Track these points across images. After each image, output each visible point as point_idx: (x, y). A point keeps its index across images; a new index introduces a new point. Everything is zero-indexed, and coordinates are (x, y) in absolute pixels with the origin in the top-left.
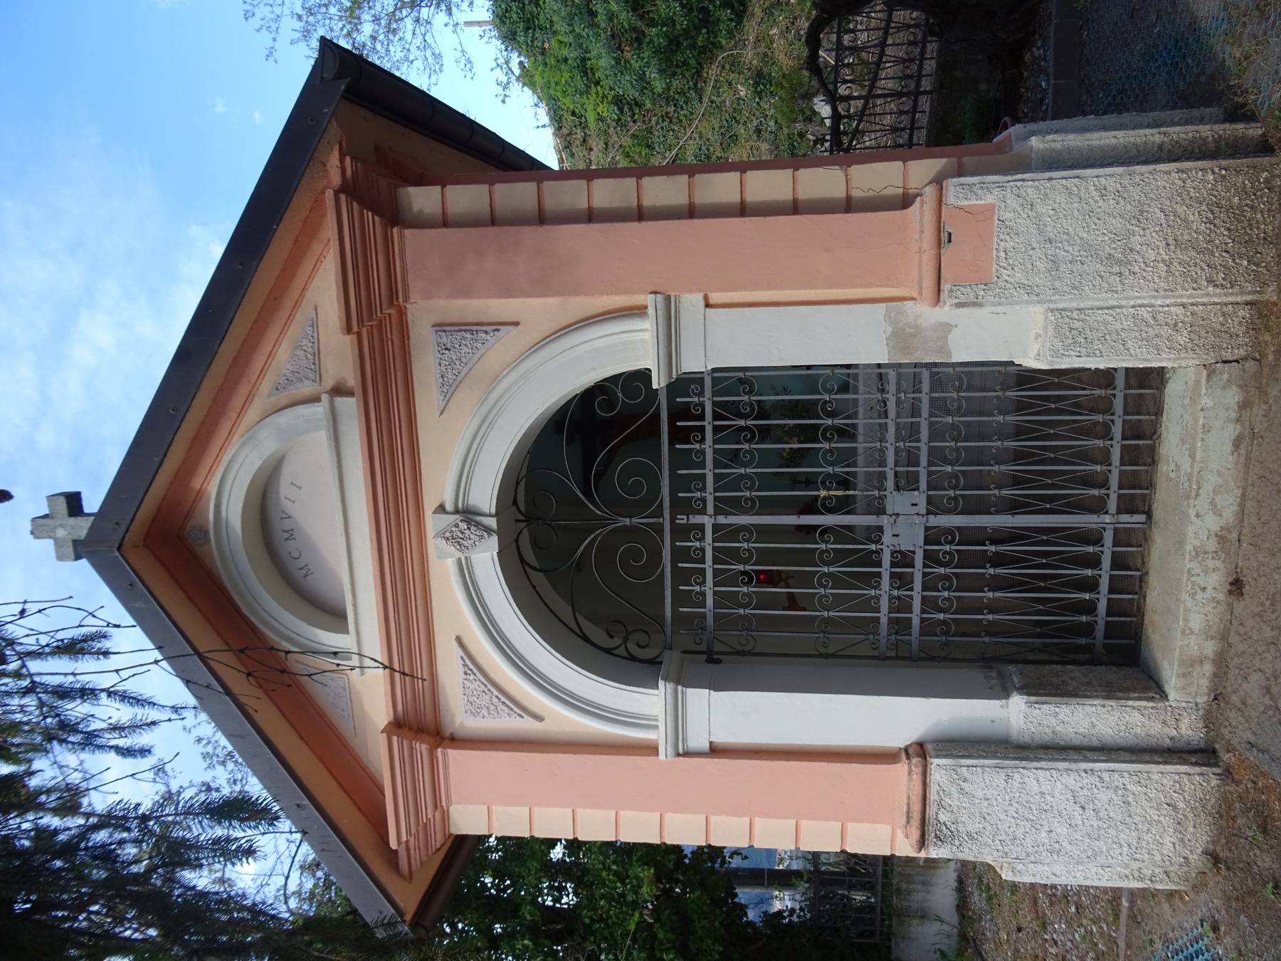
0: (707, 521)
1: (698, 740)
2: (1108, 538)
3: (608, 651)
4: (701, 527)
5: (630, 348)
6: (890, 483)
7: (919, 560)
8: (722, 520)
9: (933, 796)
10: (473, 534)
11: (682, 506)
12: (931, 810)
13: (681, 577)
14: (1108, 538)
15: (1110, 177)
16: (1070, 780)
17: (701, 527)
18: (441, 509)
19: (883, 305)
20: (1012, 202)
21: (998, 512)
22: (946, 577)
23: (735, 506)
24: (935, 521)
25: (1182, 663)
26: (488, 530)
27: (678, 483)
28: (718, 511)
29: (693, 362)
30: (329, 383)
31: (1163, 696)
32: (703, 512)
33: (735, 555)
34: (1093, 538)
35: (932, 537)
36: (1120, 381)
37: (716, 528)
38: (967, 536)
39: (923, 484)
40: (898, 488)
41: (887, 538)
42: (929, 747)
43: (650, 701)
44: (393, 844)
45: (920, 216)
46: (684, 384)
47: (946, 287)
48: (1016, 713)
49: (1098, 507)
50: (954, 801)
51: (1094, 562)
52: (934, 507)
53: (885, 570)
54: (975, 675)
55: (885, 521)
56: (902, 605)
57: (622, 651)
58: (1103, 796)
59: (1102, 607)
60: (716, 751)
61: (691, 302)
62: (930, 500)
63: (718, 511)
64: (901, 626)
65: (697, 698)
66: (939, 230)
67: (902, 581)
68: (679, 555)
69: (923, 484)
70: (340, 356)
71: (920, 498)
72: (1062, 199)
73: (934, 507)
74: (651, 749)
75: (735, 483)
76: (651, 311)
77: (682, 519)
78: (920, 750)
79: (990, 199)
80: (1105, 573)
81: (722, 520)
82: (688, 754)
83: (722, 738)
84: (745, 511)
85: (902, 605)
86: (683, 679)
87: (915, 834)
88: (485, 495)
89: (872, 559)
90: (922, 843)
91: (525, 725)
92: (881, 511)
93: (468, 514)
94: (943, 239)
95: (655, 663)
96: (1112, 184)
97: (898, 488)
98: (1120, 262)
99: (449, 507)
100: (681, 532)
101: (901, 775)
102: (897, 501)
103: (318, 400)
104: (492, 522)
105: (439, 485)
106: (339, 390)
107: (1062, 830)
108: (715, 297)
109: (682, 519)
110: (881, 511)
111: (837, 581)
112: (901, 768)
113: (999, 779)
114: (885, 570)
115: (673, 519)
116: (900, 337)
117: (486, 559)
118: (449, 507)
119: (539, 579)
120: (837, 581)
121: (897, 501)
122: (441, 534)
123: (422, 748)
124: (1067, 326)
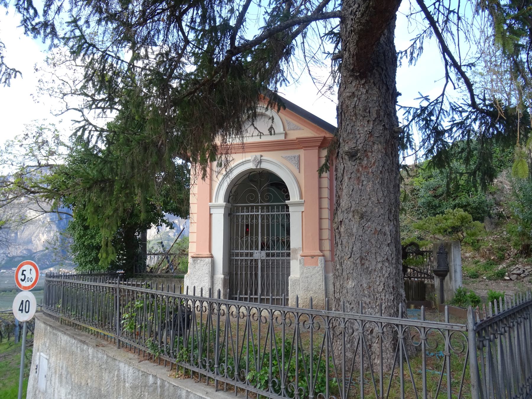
0: (259, 213)
3: (231, 192)
4: (258, 212)
5: (294, 196)
6: (268, 251)
8: (260, 216)
9: (203, 259)
10: (256, 163)
11: (263, 207)
12: (200, 259)
13: (247, 207)
14: (256, 297)
15: (323, 287)
17: (258, 212)
18: (261, 156)
20: (319, 269)
22: (248, 264)
23: (263, 219)
24: (259, 261)
26: (257, 166)
27: (268, 207)
28: (262, 215)
29: (291, 209)
30: (288, 132)
32: (261, 212)
33: (252, 219)
34: (256, 294)
35: (256, 260)
37: (258, 215)
38: (256, 268)
39: (268, 258)
40: (266, 253)
41: (256, 251)
43: (221, 201)
45: (318, 252)
50: (202, 263)
52: (262, 261)
53: (249, 251)
54: (227, 270)
56: (242, 255)
57: (231, 195)
60: (211, 215)
61: (302, 209)
63: (262, 215)
64: (237, 255)
65: (222, 211)
66: (314, 256)
67: (247, 255)
68: (252, 207)
69: (268, 258)
70: (294, 135)
71: (264, 258)
72: (319, 278)
73: (262, 261)
74: (211, 201)
75: (268, 219)
77: (260, 207)
78: (212, 257)
79: (319, 265)
81: (260, 216)
83: (213, 216)
84: (261, 221)
85: (242, 255)
86: (226, 208)
87: (195, 256)
88: (265, 166)
89: (251, 248)
90: (193, 257)
92: (262, 250)
93: (260, 162)
94: (313, 256)
95: (229, 202)
96: (321, 287)
97: (266, 253)
98: (307, 289)
99: (262, 158)
100: (257, 207)
101: (207, 253)
102: (264, 253)
103: (284, 130)
104: (258, 167)
105: (267, 156)
106: (286, 134)
108: (304, 213)
109: (260, 207)
110: (262, 250)
111: (247, 241)
112: (208, 253)
113: (207, 272)
114: (249, 251)
115: (260, 206)
116: (296, 250)
117: (251, 166)
118: (262, 158)
119: (247, 176)
120: (247, 241)
124: (296, 281)
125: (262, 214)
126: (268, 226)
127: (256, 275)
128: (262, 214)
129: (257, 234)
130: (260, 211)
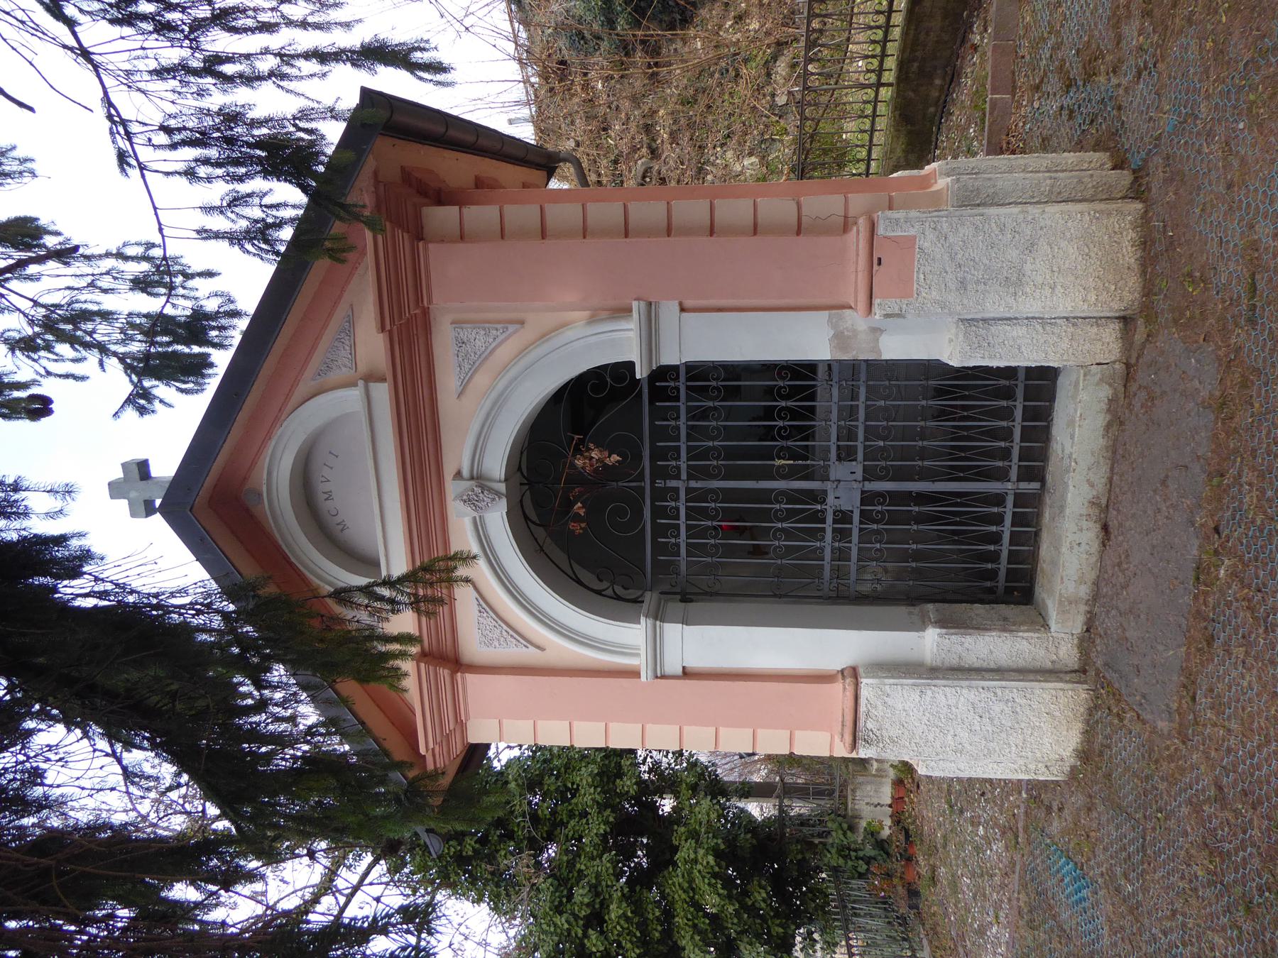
1: (673, 664)
2: (1010, 501)
3: (599, 593)
4: (676, 490)
5: (621, 343)
7: (856, 517)
8: (693, 484)
9: (862, 709)
10: (486, 497)
11: (659, 473)
13: (658, 531)
14: (1010, 501)
16: (972, 695)
17: (676, 490)
18: (458, 475)
19: (827, 313)
20: (931, 235)
21: (920, 480)
22: (878, 532)
23: (706, 474)
25: (1061, 602)
26: (498, 493)
27: (657, 454)
28: (690, 477)
29: (669, 357)
30: (362, 368)
31: (1046, 626)
32: (678, 477)
33: (704, 513)
34: (999, 500)
35: (867, 498)
36: (1021, 375)
37: (689, 490)
38: (896, 497)
39: (860, 456)
40: (839, 459)
41: (830, 499)
42: (861, 671)
44: (422, 751)
45: (856, 240)
46: (662, 373)
47: (876, 301)
48: (929, 642)
49: (1002, 475)
50: (879, 712)
51: (999, 519)
52: (869, 475)
53: (829, 526)
54: (901, 611)
55: (829, 486)
56: (841, 555)
57: (609, 592)
58: (997, 707)
59: (1004, 555)
60: (687, 674)
61: (669, 310)
62: (865, 469)
63: (690, 477)
64: (839, 573)
65: (672, 631)
67: (842, 534)
68: (658, 512)
69: (860, 456)
70: (371, 344)
71: (858, 468)
73: (869, 475)
74: (634, 674)
76: (635, 314)
77: (660, 483)
78: (853, 673)
79: (912, 232)
80: (1007, 528)
81: (693, 484)
82: (663, 677)
83: (694, 663)
85: (841, 555)
86: (659, 616)
87: (848, 738)
88: (496, 464)
89: (819, 517)
90: (854, 746)
91: (527, 655)
92: (825, 478)
94: (874, 261)
95: (637, 601)
97: (839, 459)
99: (466, 473)
100: (659, 494)
101: (838, 693)
103: (355, 385)
104: (502, 487)
105: (457, 456)
106: (370, 378)
107: (964, 735)
108: (689, 303)
109: (660, 483)
110: (825, 478)
111: (789, 534)
112: (838, 686)
113: (915, 695)
114: (829, 526)
115: (653, 482)
117: (497, 519)
118: (466, 473)
119: (540, 533)
120: (789, 534)
121: (839, 470)
122: (459, 497)
123: (444, 673)
125: (684, 476)
126: (731, 454)
127: (922, 498)
128: (684, 476)
129: (764, 496)
130: (673, 483)
